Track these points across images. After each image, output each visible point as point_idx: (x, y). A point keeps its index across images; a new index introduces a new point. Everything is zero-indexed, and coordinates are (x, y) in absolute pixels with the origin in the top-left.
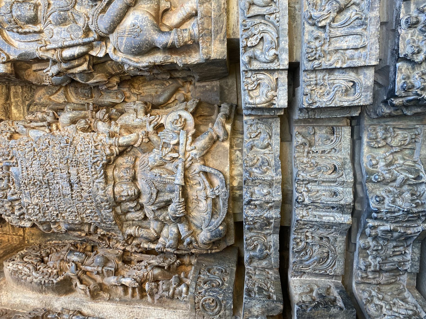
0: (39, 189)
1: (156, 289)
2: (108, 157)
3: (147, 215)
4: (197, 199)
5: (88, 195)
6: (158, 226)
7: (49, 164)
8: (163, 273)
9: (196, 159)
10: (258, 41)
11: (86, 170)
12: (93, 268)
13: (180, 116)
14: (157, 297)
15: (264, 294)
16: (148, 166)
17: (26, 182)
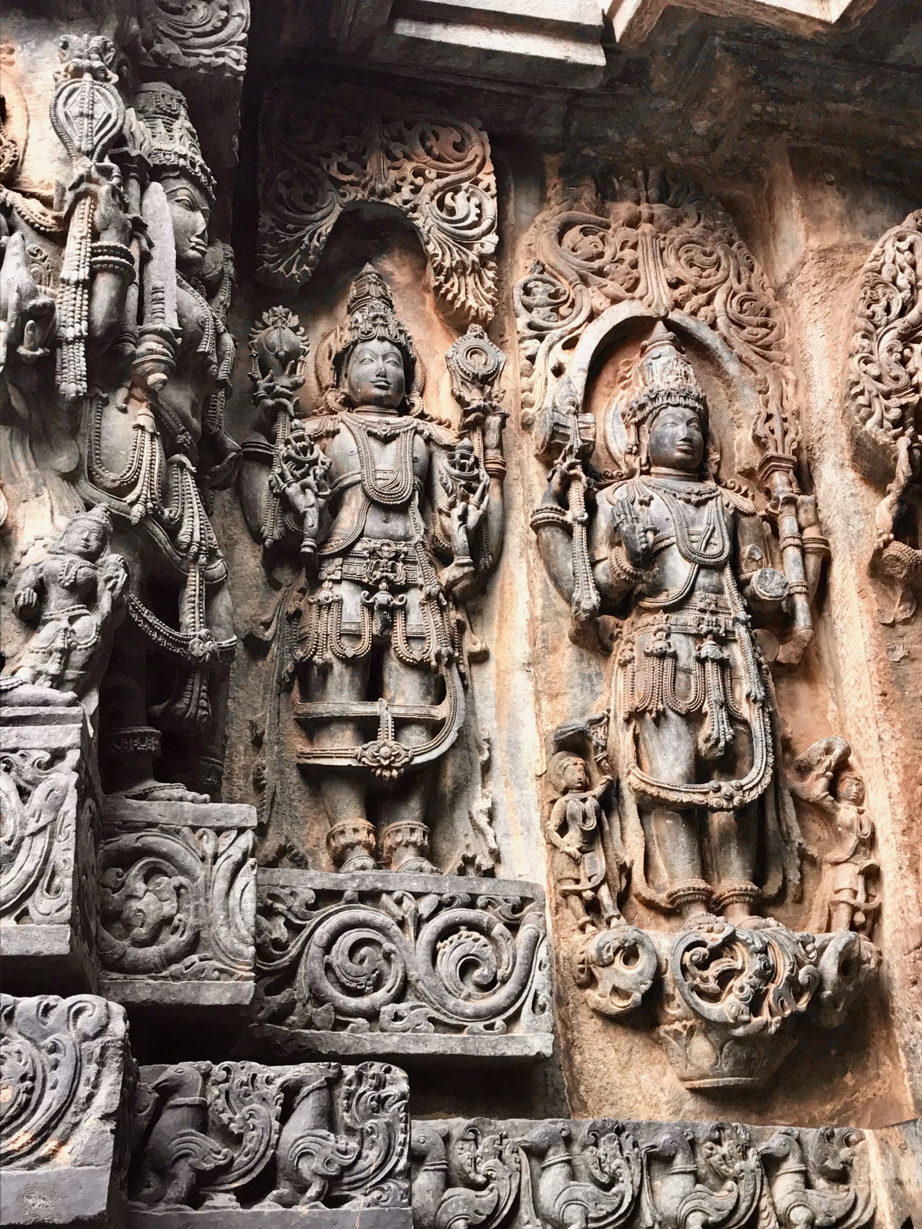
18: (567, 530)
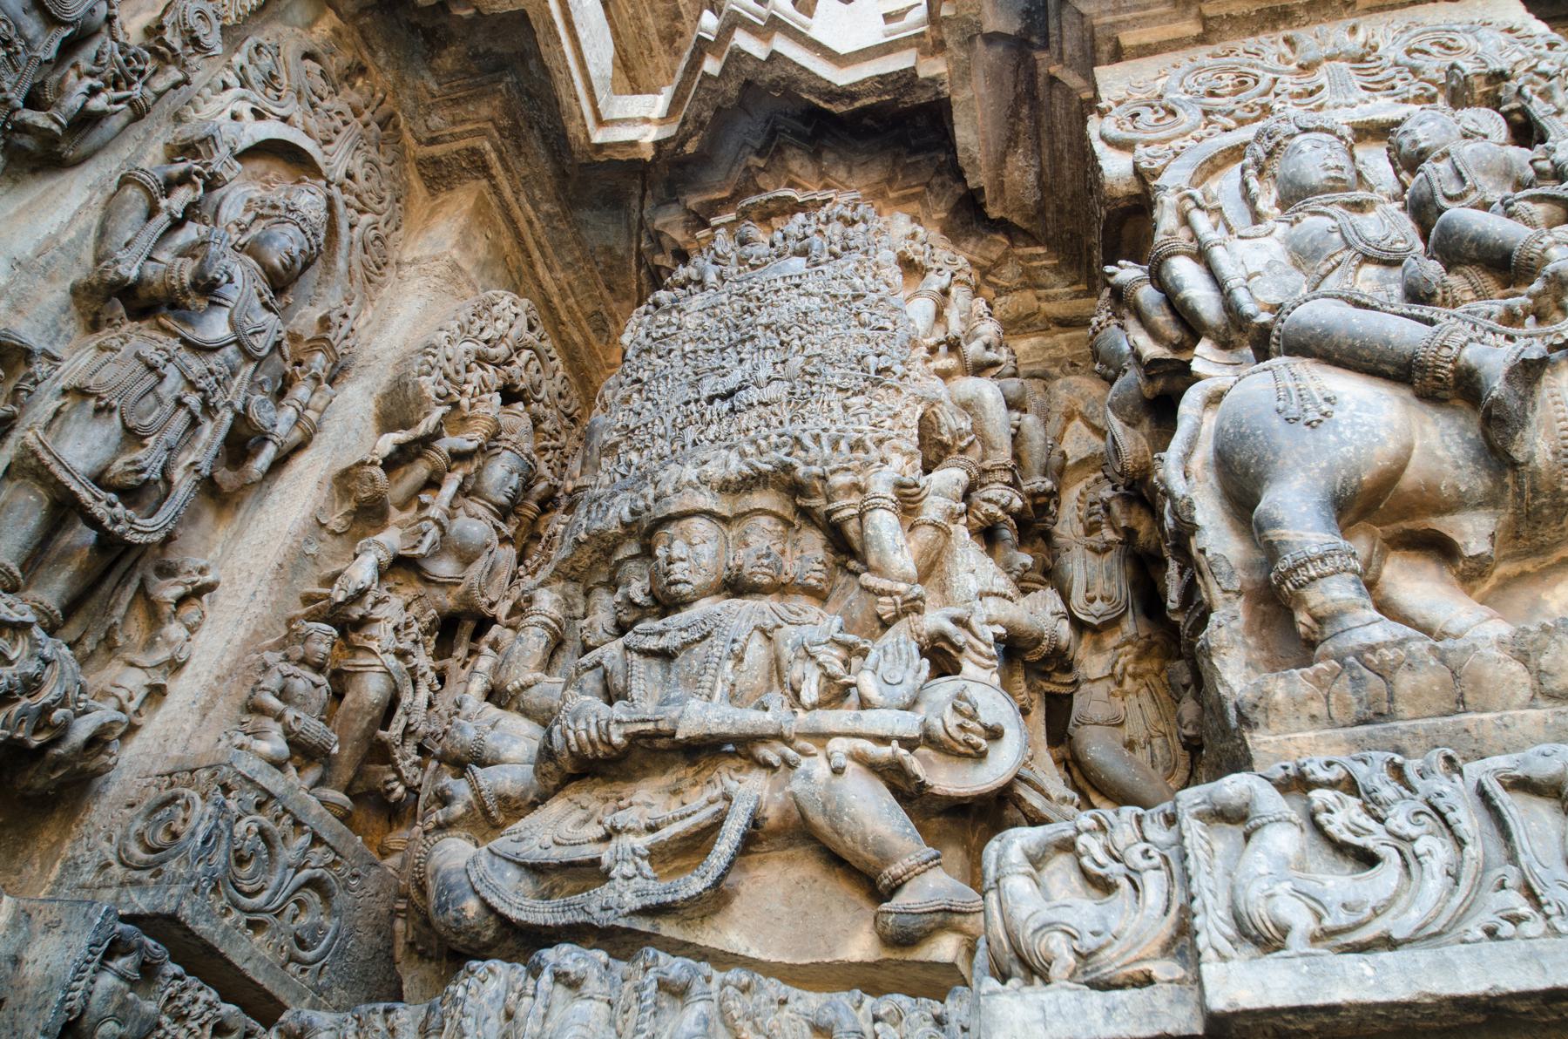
1: (299, 655)
2: (818, 484)
5: (689, 440)
9: (789, 782)
10: (1348, 837)
11: (774, 421)
13: (995, 734)
14: (273, 658)
15: (101, 1020)
18: (152, 212)
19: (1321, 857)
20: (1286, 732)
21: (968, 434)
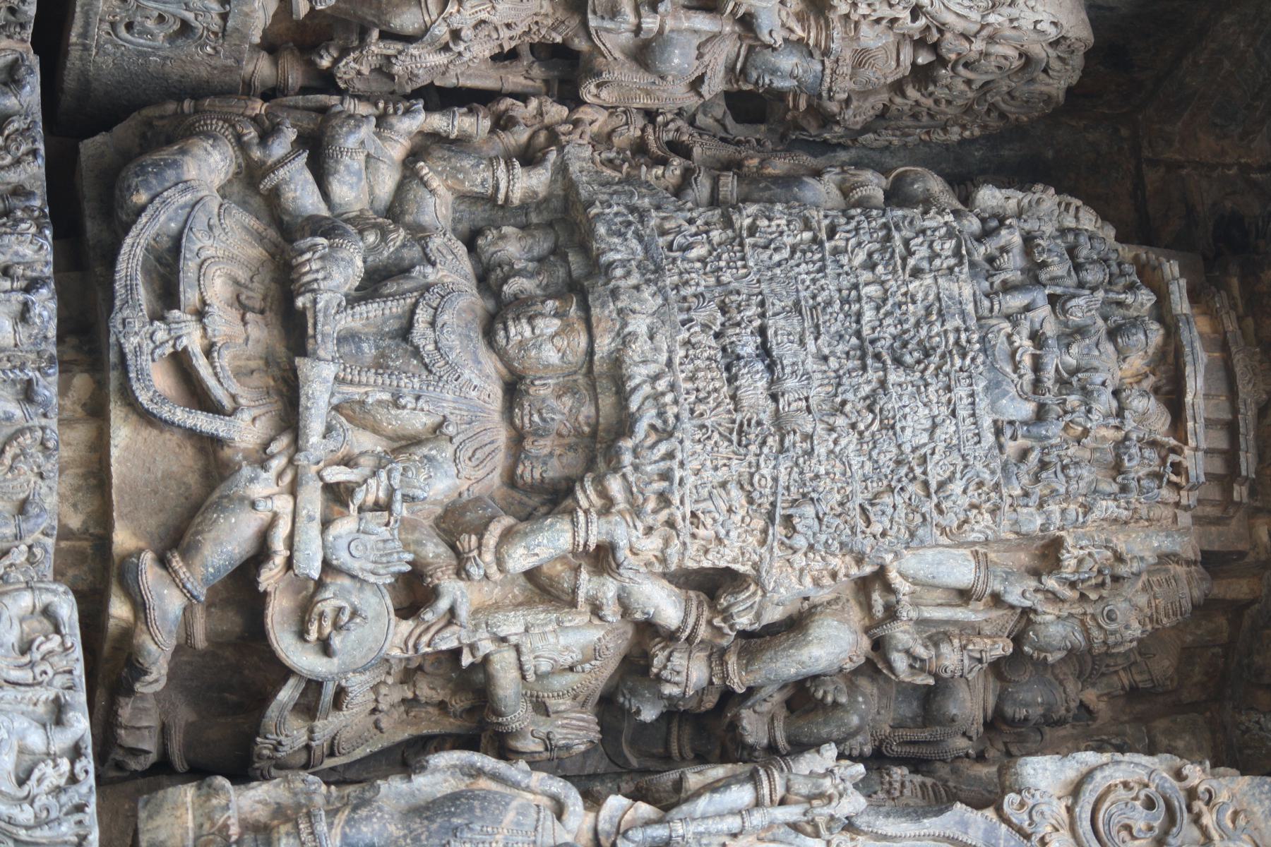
0: (905, 332)
3: (461, 249)
4: (244, 308)
6: (412, 208)
7: (861, 433)
8: (380, 12)
9: (250, 464)
10: (36, 774)
11: (700, 408)
12: (686, 25)
13: (325, 648)
16: (456, 441)
17: (958, 362)
19: (27, 758)
20: (194, 810)
21: (732, 627)
